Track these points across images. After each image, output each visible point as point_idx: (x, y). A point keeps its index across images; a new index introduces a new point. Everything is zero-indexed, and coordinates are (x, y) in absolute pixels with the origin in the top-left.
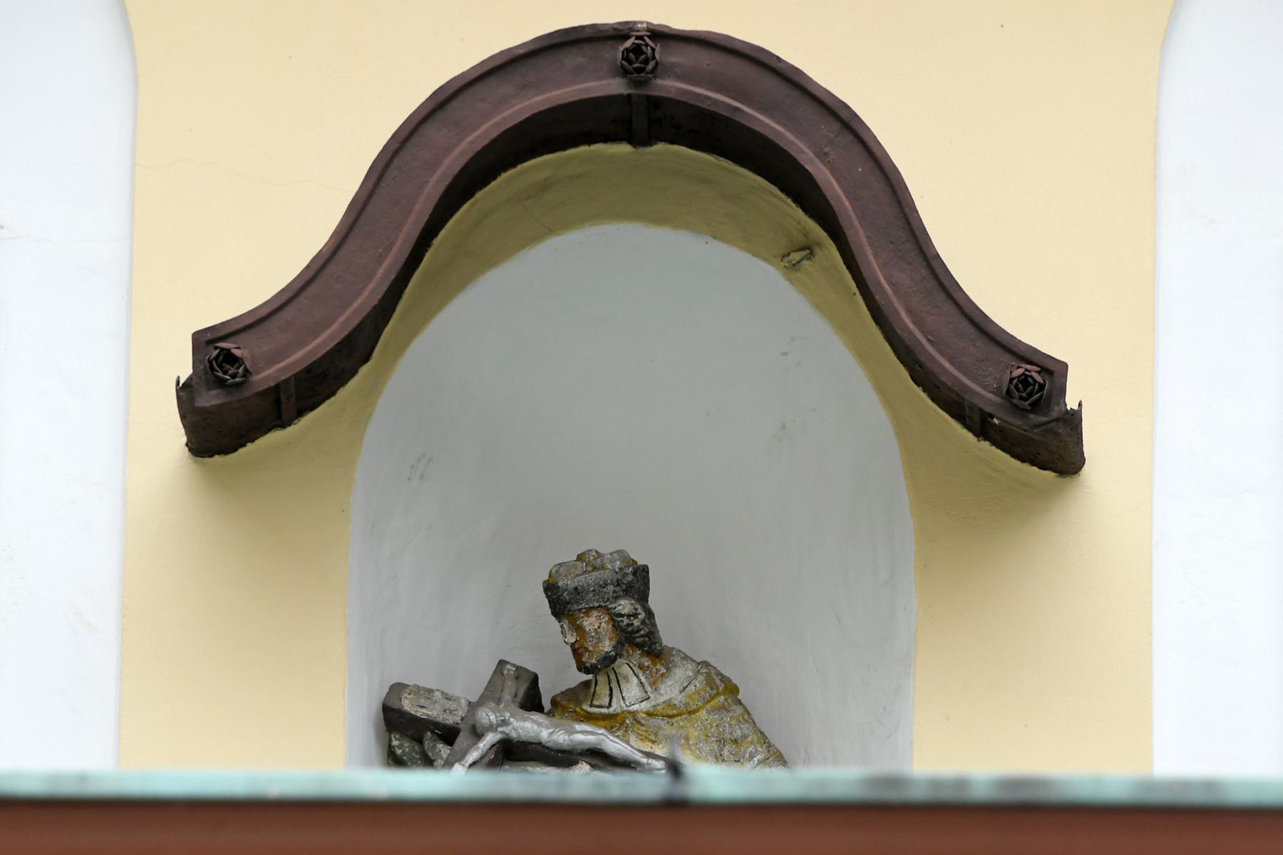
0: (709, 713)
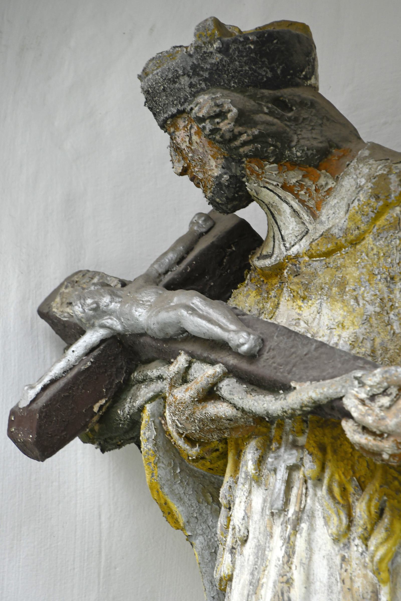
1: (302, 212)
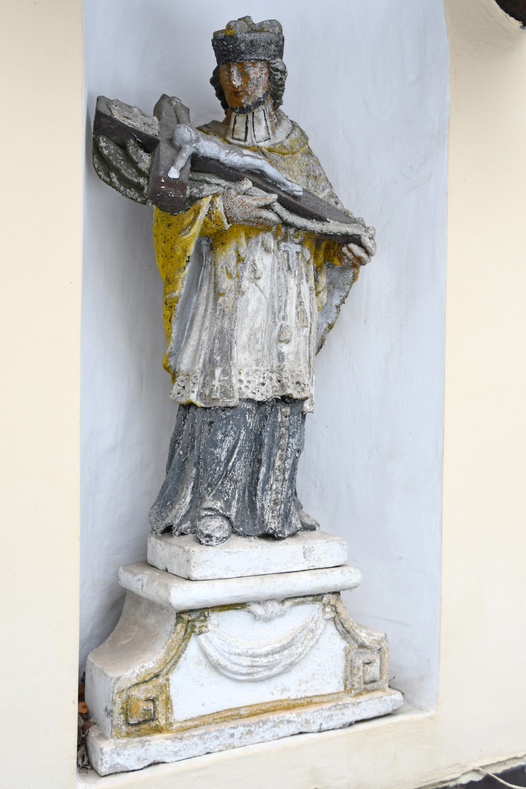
0: (302, 155)
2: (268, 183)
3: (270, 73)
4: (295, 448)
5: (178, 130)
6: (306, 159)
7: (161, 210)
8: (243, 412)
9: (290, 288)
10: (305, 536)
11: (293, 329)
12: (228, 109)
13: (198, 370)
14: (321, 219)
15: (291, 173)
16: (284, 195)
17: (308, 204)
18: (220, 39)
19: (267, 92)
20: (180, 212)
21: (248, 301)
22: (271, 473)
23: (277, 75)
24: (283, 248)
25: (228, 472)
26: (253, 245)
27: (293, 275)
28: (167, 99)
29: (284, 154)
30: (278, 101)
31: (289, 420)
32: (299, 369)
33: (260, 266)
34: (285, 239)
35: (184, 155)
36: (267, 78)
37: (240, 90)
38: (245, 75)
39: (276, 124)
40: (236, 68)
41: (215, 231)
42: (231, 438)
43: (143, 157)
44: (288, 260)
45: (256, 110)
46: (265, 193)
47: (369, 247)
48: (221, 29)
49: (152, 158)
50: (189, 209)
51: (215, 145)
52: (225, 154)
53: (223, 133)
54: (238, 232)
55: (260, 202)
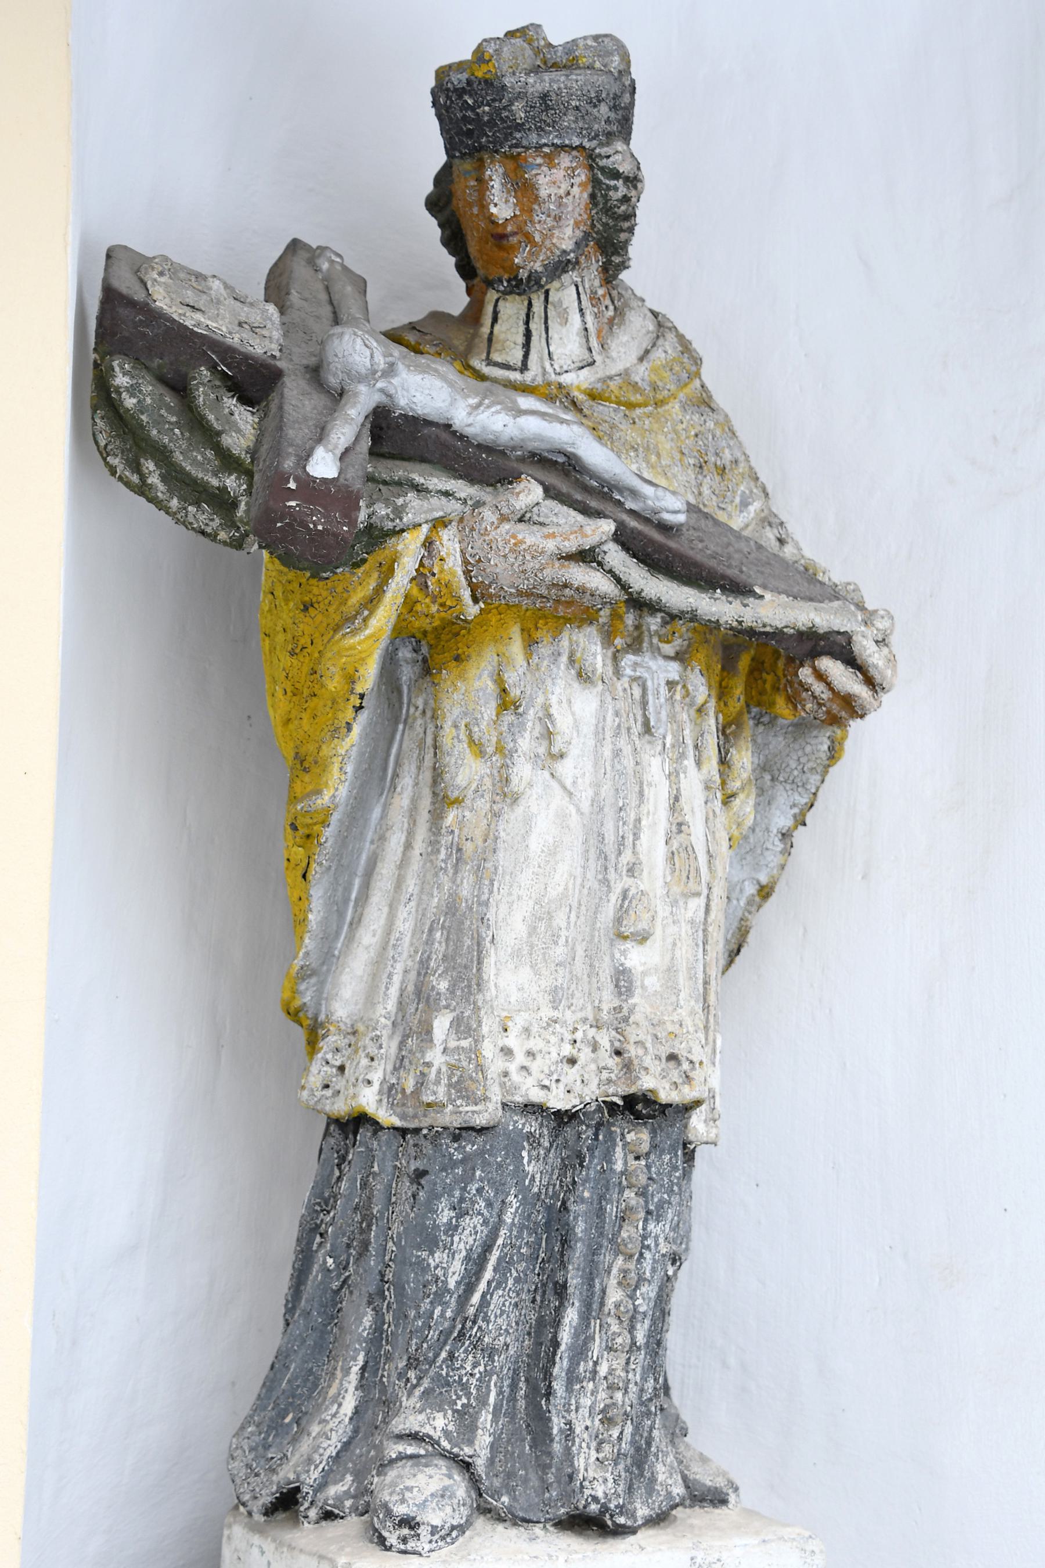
1: (593, 335)
2: (586, 489)
3: (595, 182)
4: (664, 1251)
5: (336, 342)
6: (696, 417)
7: (284, 564)
8: (514, 1144)
9: (650, 785)
10: (695, 1522)
11: (658, 902)
12: (476, 281)
13: (383, 1020)
14: (738, 589)
15: (653, 458)
16: (633, 523)
17: (700, 546)
18: (456, 90)
19: (587, 235)
20: (339, 570)
21: (528, 821)
22: (595, 1325)
23: (616, 189)
24: (628, 672)
25: (469, 1324)
26: (545, 663)
27: (660, 748)
28: (303, 255)
29: (631, 406)
30: (616, 259)
31: (648, 1167)
32: (676, 1018)
33: (563, 722)
34: (635, 645)
35: (352, 412)
36: (585, 195)
37: (509, 229)
38: (524, 190)
39: (611, 322)
40: (501, 170)
41: (437, 623)
42: (478, 1220)
43: (237, 416)
44: (644, 704)
45: (556, 284)
46: (580, 518)
47: (876, 667)
48: (457, 59)
49: (261, 419)
50: (364, 561)
51: (438, 383)
52: (468, 409)
53: (462, 348)
54: (502, 623)
55: (566, 543)
